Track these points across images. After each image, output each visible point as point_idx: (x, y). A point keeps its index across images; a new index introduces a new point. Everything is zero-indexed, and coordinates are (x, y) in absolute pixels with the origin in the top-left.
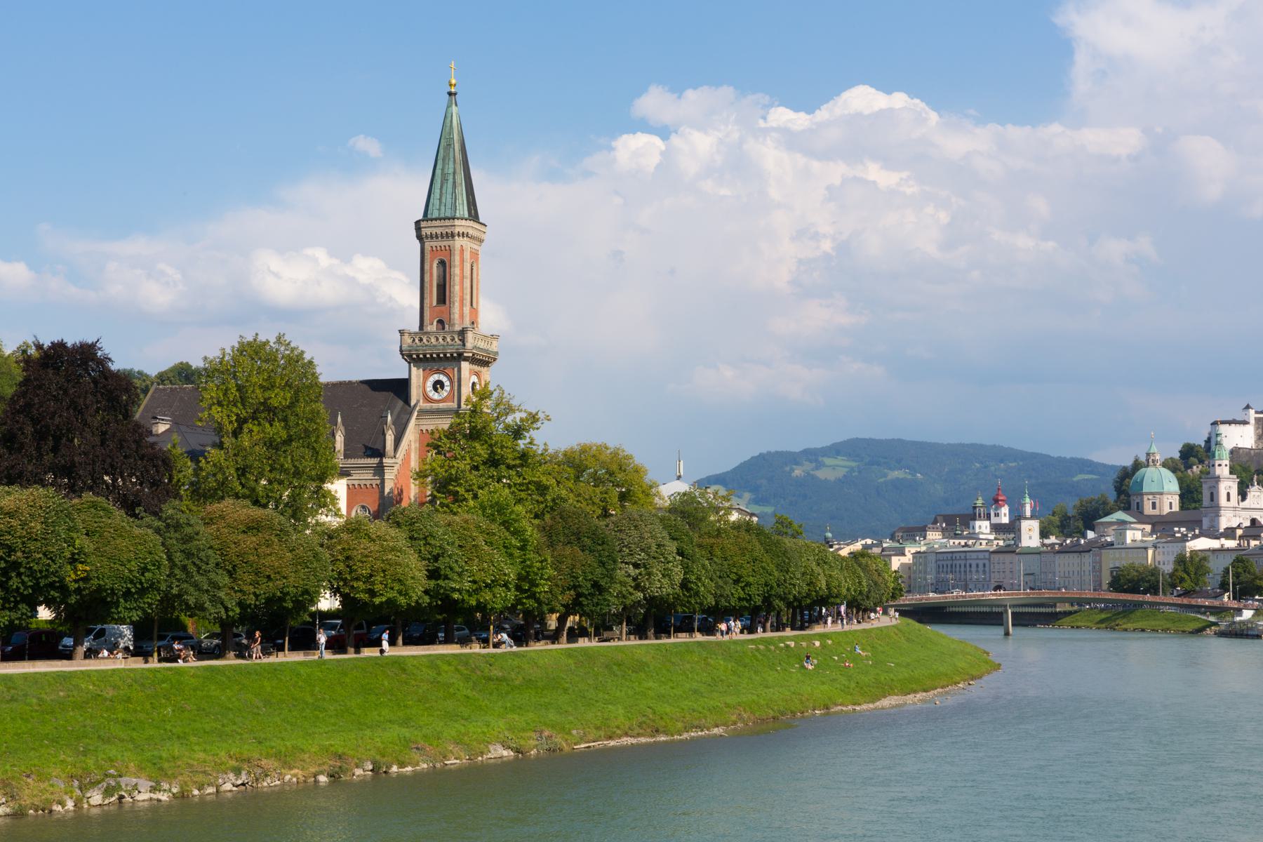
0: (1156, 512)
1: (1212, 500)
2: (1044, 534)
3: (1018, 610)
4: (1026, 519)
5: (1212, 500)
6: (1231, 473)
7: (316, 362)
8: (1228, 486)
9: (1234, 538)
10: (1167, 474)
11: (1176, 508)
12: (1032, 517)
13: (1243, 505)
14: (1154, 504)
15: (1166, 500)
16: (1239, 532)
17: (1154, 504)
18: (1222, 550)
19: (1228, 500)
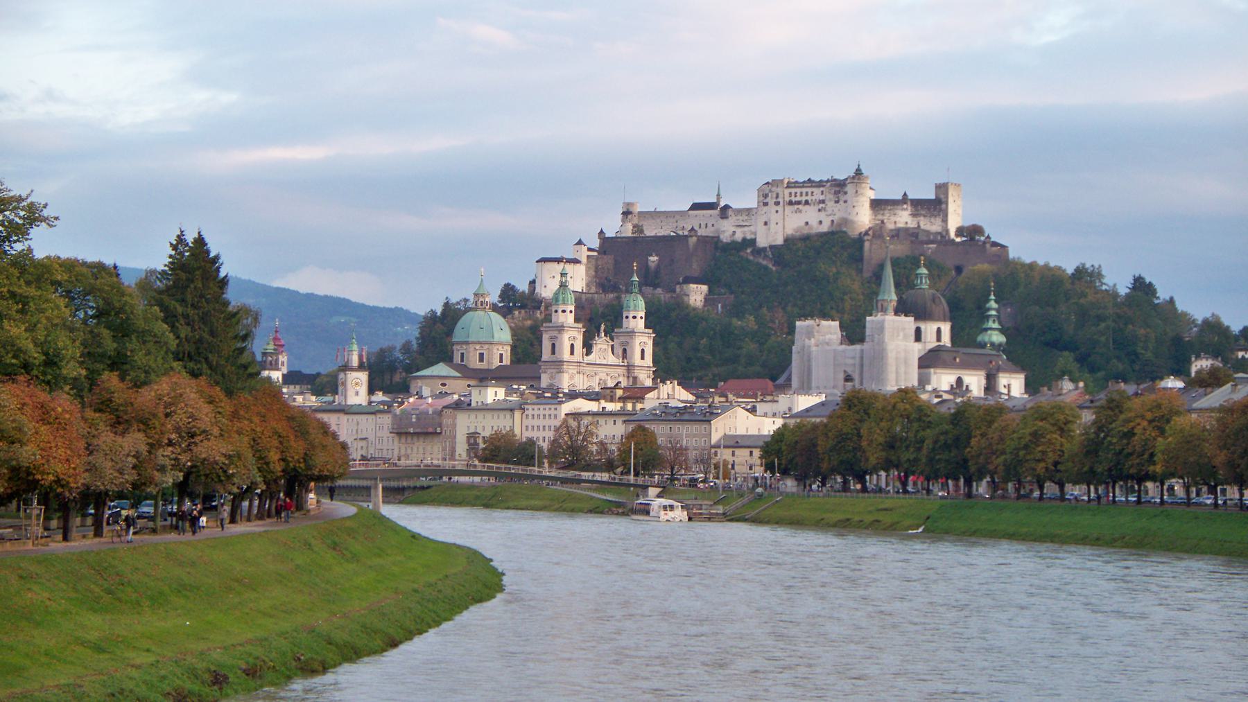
0: (484, 366)
1: (553, 352)
2: (371, 391)
3: (387, 484)
4: (352, 370)
5: (553, 352)
6: (577, 320)
7: (1104, 273)
8: (572, 335)
9: (612, 400)
10: (496, 317)
11: (507, 361)
12: (361, 367)
13: (588, 359)
14: (481, 355)
15: (497, 351)
16: (619, 393)
17: (481, 355)
18: (603, 413)
19: (643, 358)
